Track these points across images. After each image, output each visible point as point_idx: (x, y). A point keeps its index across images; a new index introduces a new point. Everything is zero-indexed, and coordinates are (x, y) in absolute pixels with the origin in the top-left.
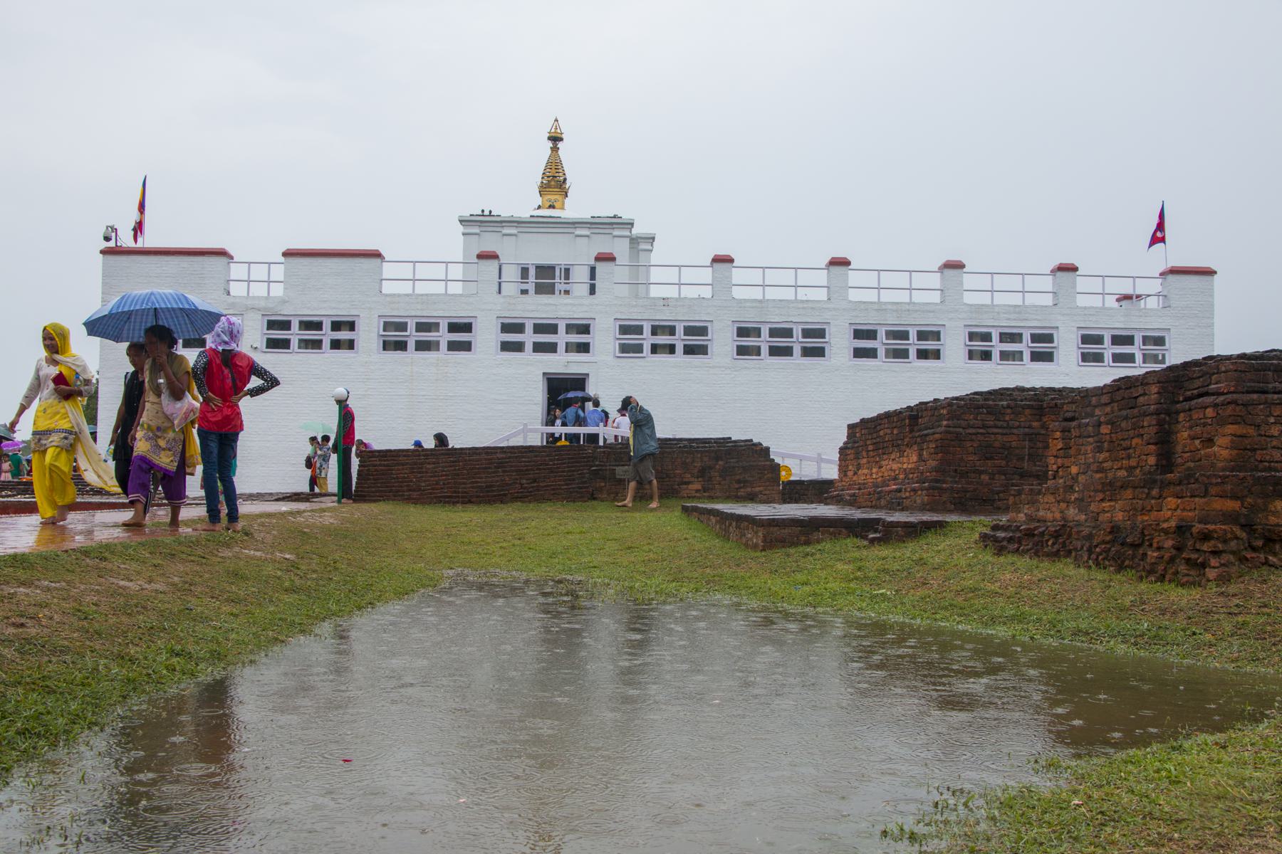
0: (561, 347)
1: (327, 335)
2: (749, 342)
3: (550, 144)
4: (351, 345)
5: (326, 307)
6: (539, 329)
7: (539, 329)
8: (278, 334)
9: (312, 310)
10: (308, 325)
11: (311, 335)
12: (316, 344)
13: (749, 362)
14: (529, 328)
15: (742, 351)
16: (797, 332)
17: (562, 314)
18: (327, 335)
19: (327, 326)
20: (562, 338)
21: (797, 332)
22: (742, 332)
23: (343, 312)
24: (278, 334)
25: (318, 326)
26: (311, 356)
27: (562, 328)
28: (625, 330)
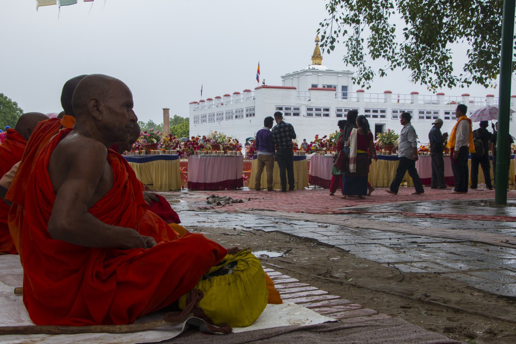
0: (379, 116)
1: (322, 112)
2: (421, 115)
3: (316, 43)
4: (327, 115)
5: (322, 105)
6: (374, 111)
7: (374, 111)
8: (310, 112)
9: (318, 106)
10: (317, 110)
11: (318, 112)
12: (319, 115)
13: (421, 120)
14: (371, 111)
15: (420, 118)
16: (432, 112)
17: (379, 107)
18: (322, 112)
19: (322, 110)
20: (379, 114)
21: (432, 112)
22: (420, 113)
23: (326, 106)
24: (310, 112)
25: (320, 110)
26: (318, 118)
27: (379, 111)
28: (394, 112)
